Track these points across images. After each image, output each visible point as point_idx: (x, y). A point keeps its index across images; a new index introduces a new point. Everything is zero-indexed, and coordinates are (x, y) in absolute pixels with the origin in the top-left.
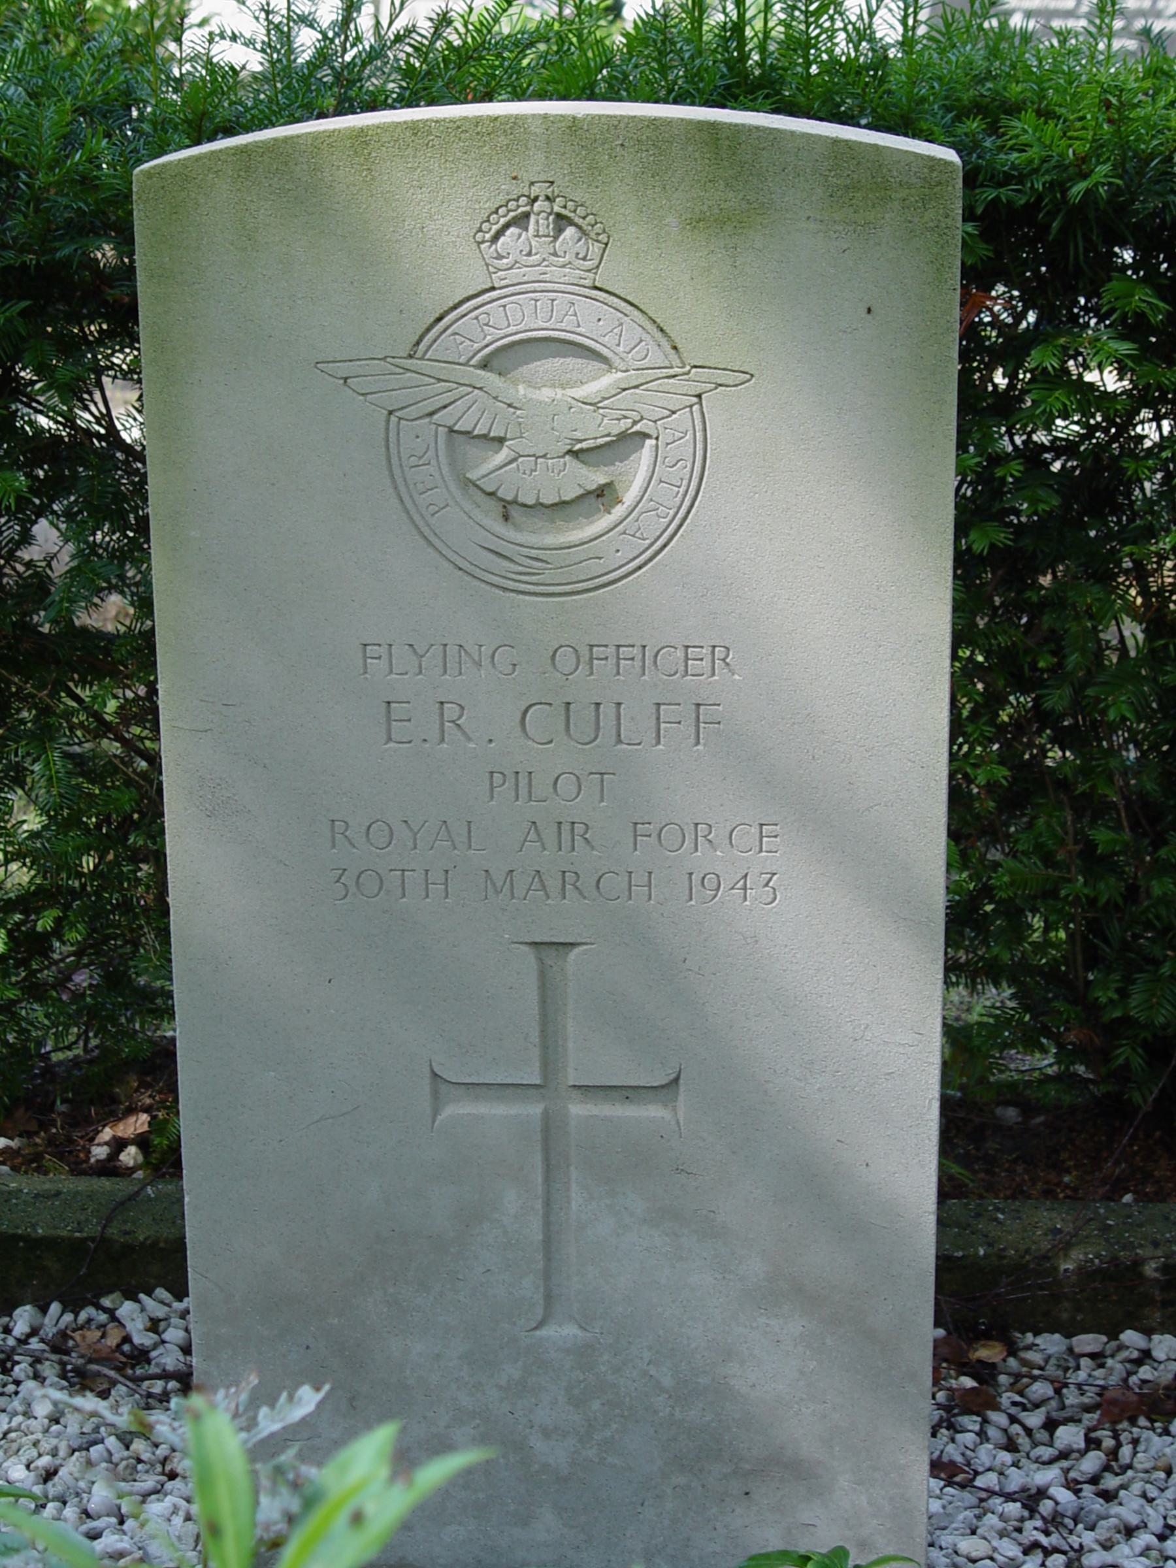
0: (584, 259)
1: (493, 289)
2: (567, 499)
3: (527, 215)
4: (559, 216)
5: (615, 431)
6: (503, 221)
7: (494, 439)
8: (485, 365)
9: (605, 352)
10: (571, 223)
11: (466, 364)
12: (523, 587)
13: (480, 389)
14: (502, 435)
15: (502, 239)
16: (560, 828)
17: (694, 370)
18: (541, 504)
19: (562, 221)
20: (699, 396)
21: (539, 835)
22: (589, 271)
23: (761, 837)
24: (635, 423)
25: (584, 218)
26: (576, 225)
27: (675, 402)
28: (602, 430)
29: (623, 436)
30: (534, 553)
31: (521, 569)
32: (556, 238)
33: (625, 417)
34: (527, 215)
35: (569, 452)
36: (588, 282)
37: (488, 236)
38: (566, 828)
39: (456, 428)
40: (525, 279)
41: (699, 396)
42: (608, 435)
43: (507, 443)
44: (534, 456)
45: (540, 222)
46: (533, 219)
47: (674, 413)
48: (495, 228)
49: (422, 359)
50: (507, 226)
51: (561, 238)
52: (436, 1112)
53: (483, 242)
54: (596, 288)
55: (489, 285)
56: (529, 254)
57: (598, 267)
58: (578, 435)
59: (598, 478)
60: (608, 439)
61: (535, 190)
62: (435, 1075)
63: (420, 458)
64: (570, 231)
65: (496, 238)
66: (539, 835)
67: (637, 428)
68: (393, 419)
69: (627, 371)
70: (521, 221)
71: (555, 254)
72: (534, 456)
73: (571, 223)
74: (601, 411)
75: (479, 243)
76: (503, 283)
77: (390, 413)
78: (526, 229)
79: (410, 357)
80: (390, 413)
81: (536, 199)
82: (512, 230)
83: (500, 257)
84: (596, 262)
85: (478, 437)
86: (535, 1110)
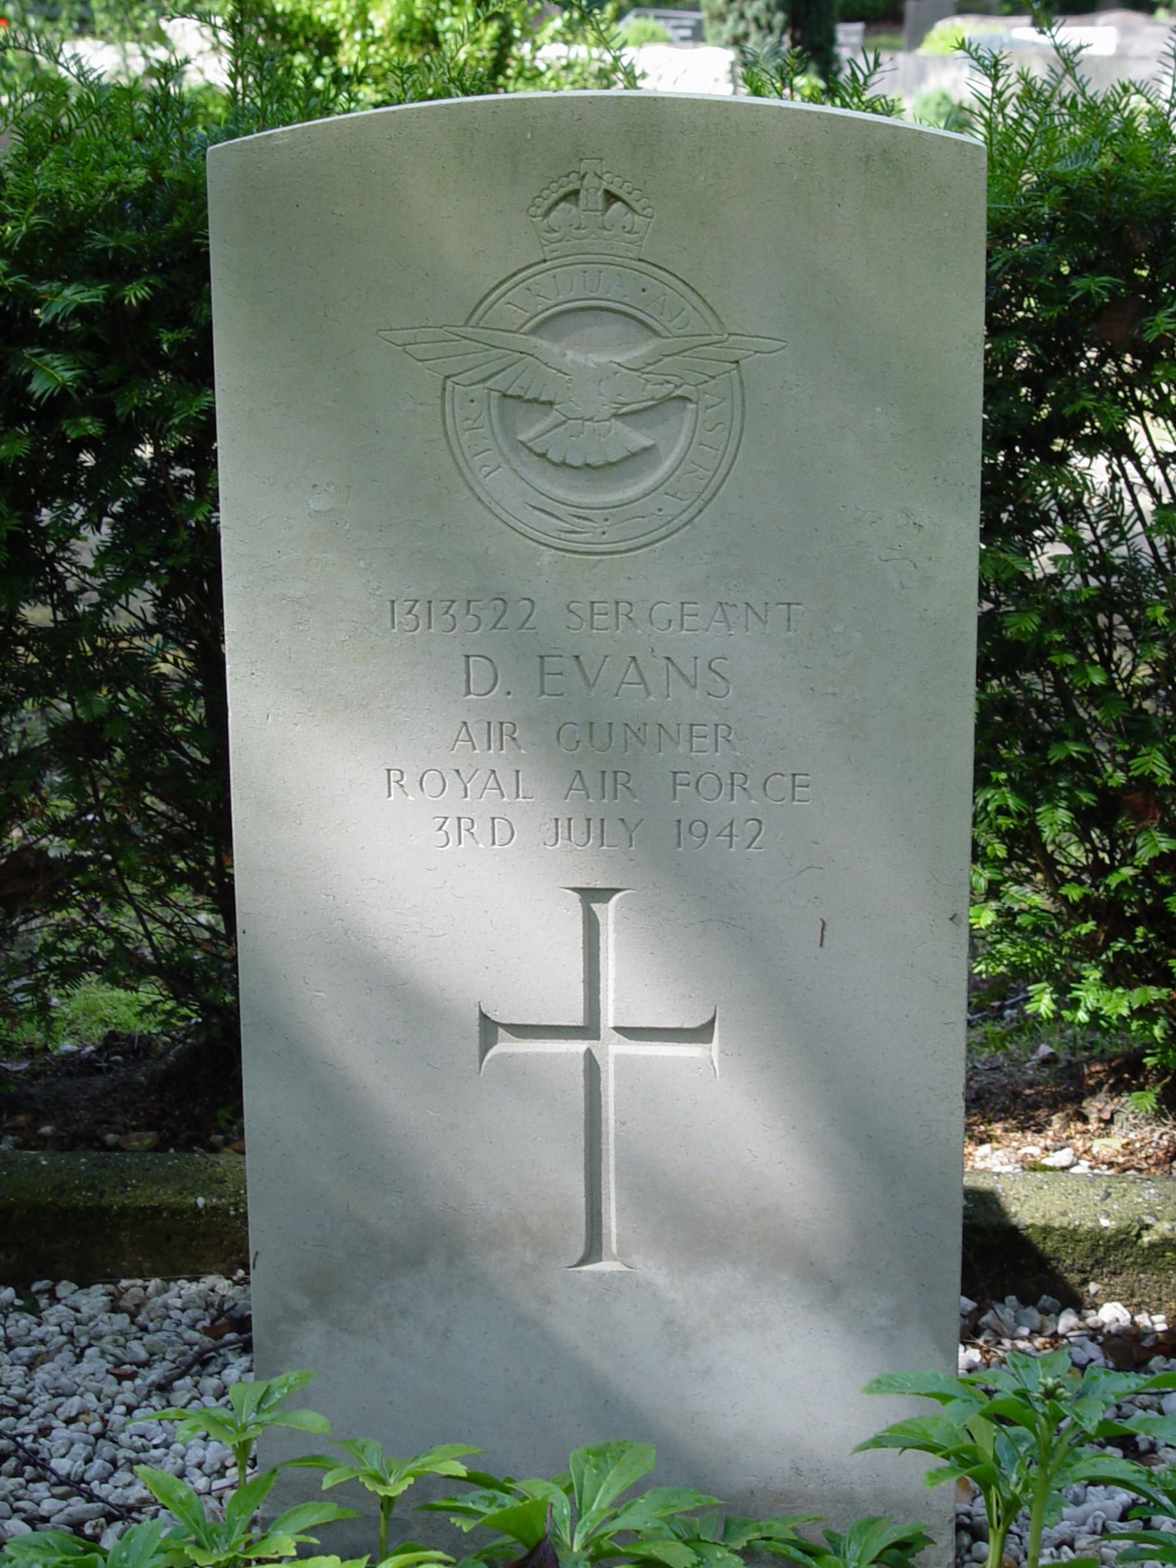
1: (545, 261)
2: (613, 460)
3: (576, 193)
4: (607, 192)
6: (555, 196)
7: (543, 403)
10: (617, 198)
12: (573, 546)
13: (532, 355)
14: (552, 399)
15: (554, 213)
16: (603, 778)
17: (733, 338)
18: (588, 465)
19: (611, 197)
21: (583, 783)
23: (794, 786)
24: (677, 387)
25: (630, 193)
26: (624, 202)
29: (668, 399)
30: (581, 512)
33: (669, 382)
34: (576, 193)
35: (615, 415)
37: (540, 211)
38: (609, 777)
39: (509, 392)
42: (652, 399)
43: (556, 407)
44: (581, 418)
45: (592, 197)
46: (582, 192)
50: (556, 204)
52: (484, 1051)
54: (640, 260)
55: (542, 257)
56: (578, 228)
58: (623, 399)
59: (641, 440)
60: (650, 403)
62: (484, 1017)
63: (475, 421)
64: (617, 206)
66: (583, 783)
67: (678, 392)
68: (449, 383)
72: (581, 418)
73: (617, 198)
74: (645, 376)
76: (555, 254)
77: (448, 377)
79: (466, 324)
80: (448, 377)
82: (562, 205)
85: (528, 401)
86: (579, 1047)
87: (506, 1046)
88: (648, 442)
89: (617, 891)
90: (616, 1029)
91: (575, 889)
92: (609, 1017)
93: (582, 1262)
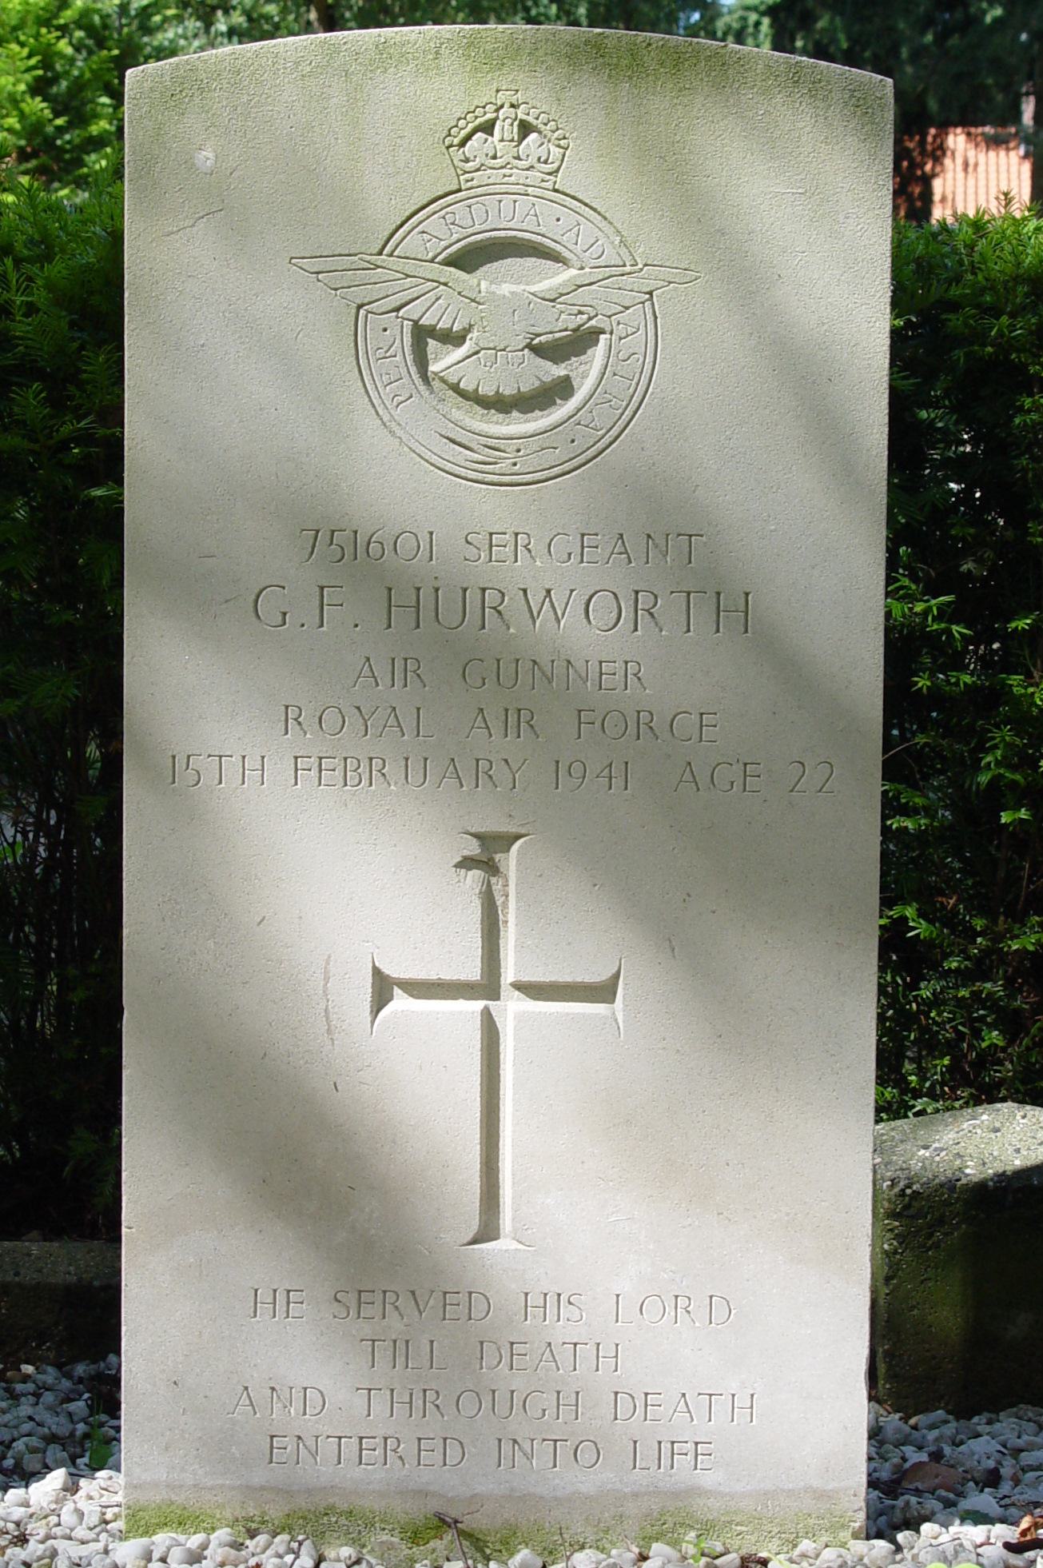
0: (546, 162)
5: (572, 326)
8: (450, 262)
9: (566, 254)
11: (432, 261)
13: (445, 284)
19: (525, 129)
20: (651, 293)
22: (550, 174)
24: (590, 319)
26: (540, 132)
27: (627, 298)
28: (560, 325)
31: (476, 456)
32: (520, 142)
36: (549, 185)
37: (456, 141)
40: (491, 181)
41: (651, 293)
45: (505, 129)
46: (498, 123)
47: (627, 308)
48: (463, 133)
49: (391, 255)
51: (525, 143)
53: (451, 146)
55: (455, 187)
56: (494, 157)
57: (557, 171)
61: (501, 98)
62: (377, 972)
64: (534, 136)
65: (463, 144)
67: (593, 322)
68: (362, 312)
69: (582, 268)
70: (488, 128)
71: (518, 158)
75: (448, 148)
76: (469, 184)
78: (492, 135)
80: (360, 307)
81: (502, 107)
83: (467, 160)
84: (556, 165)
86: (478, 1005)
87: (401, 1003)
88: (563, 373)
89: (518, 837)
90: (518, 986)
91: (476, 836)
92: (509, 973)
93: (474, 1242)
